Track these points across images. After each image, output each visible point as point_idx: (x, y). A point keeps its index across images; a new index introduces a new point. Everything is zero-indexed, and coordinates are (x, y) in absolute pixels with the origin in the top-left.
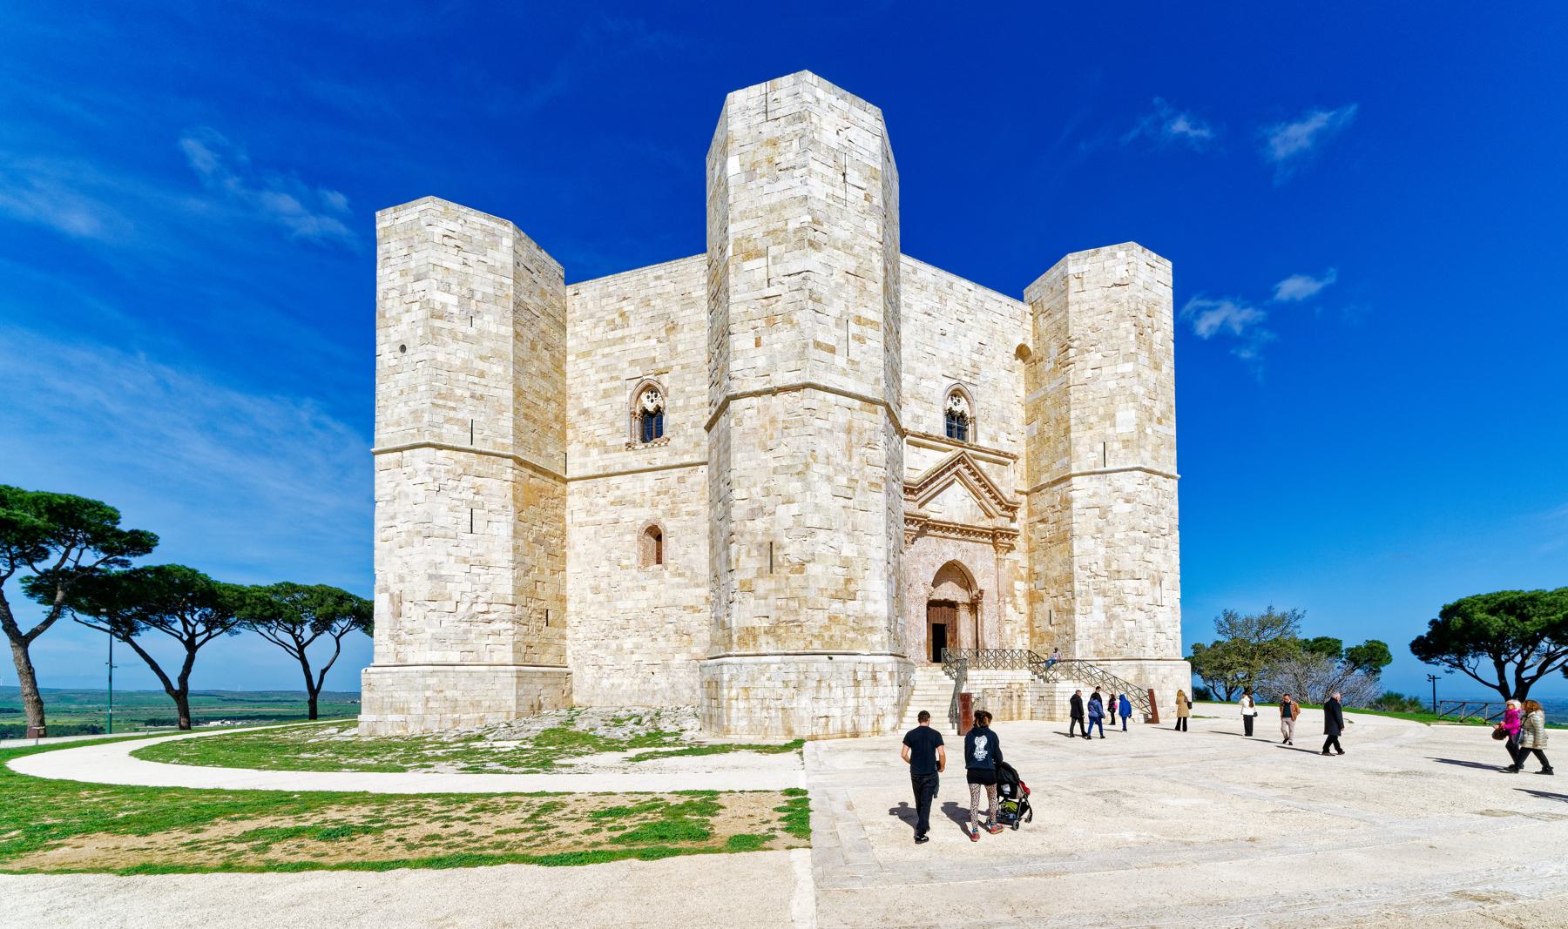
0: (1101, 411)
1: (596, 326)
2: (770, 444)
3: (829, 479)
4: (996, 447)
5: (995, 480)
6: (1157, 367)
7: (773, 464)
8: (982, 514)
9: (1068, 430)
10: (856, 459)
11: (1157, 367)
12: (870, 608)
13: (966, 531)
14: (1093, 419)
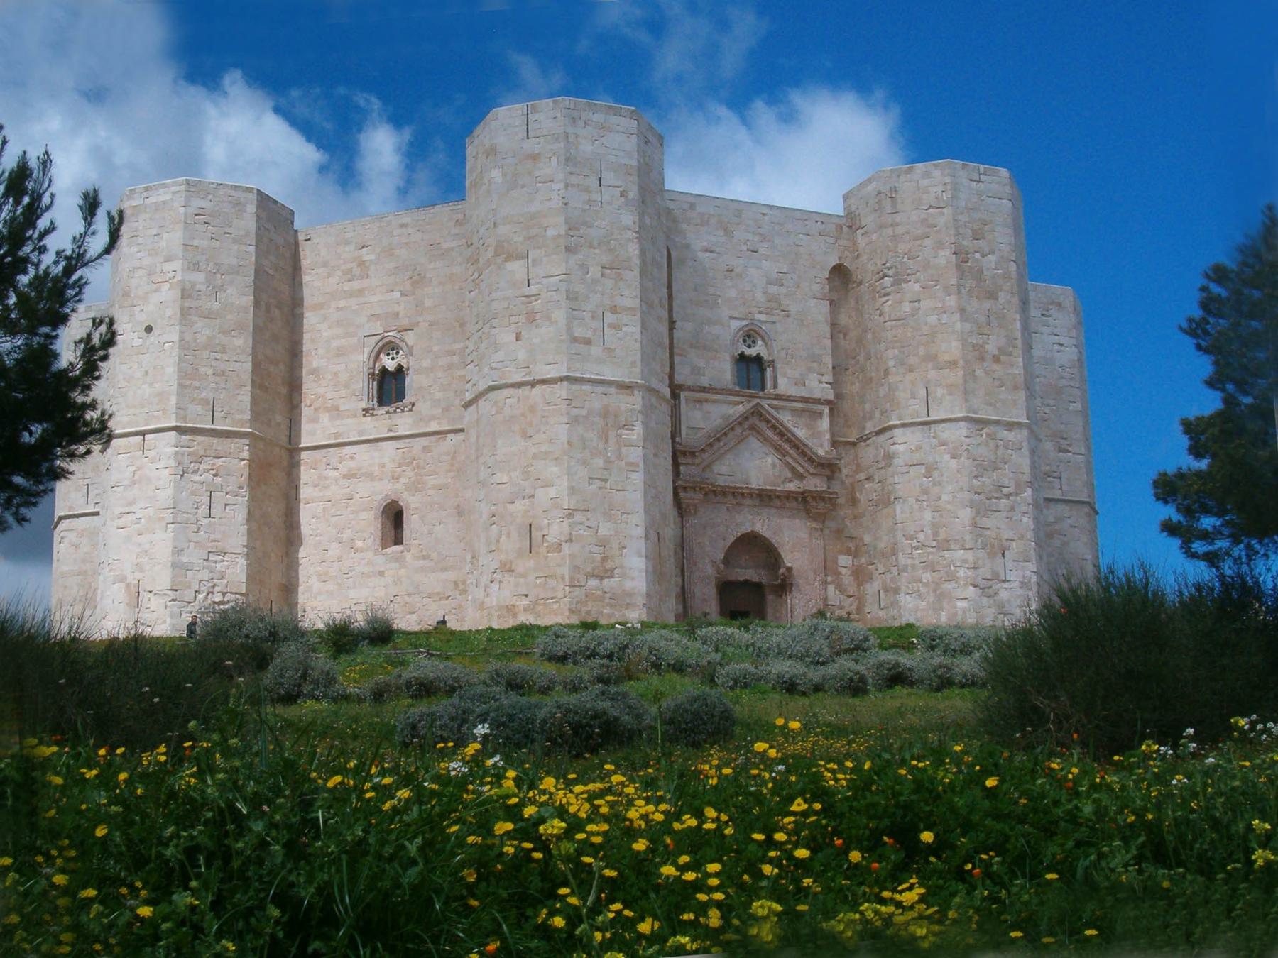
0: (922, 351)
1: (329, 275)
2: (530, 431)
3: (585, 463)
4: (803, 394)
5: (801, 433)
6: (992, 296)
7: (534, 450)
8: (790, 475)
9: (887, 373)
10: (612, 440)
11: (992, 296)
12: (628, 585)
13: (765, 498)
14: (913, 360)
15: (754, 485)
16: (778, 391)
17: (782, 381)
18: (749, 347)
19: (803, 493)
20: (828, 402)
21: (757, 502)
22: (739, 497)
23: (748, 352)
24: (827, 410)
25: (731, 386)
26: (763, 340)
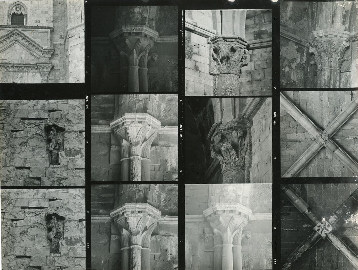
8: (33, 58)
15: (16, 62)
16: (27, 25)
17: (29, 21)
18: (18, 11)
19: (36, 64)
20: (49, 28)
21: (16, 69)
22: (8, 68)
23: (16, 12)
24: (49, 30)
25: (6, 24)
26: (23, 8)
